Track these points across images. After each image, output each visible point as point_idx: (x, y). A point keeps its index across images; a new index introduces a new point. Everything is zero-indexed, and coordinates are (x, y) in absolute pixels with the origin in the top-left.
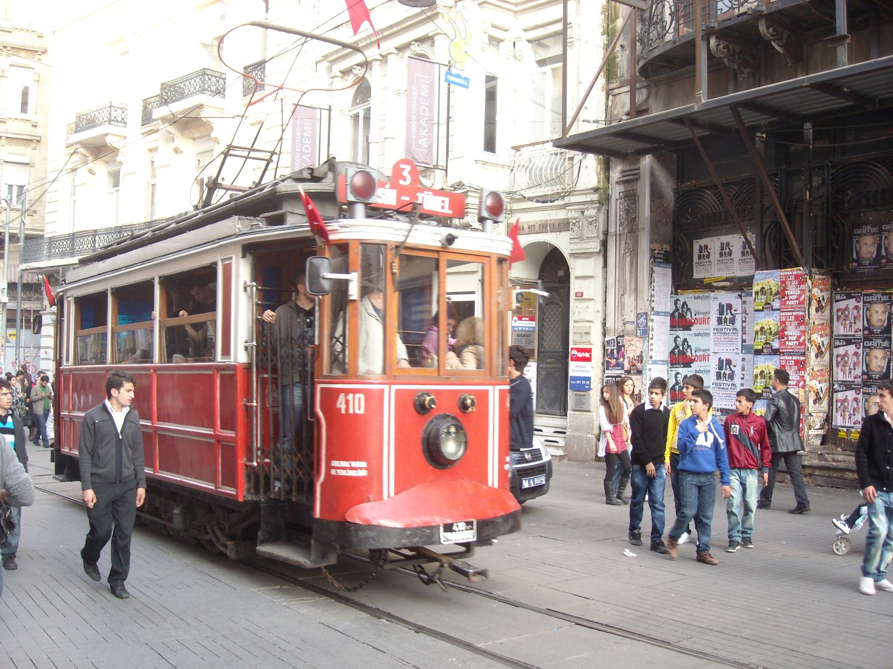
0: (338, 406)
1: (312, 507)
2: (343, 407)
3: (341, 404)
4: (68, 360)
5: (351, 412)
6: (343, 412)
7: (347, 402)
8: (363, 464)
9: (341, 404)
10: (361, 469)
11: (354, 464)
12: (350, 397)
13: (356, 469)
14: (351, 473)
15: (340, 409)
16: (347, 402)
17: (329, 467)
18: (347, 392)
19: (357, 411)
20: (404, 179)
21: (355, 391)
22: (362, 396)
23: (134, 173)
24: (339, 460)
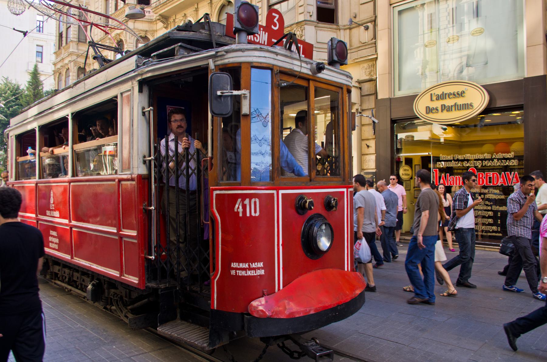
0: (236, 210)
1: (210, 297)
2: (241, 210)
3: (238, 208)
4: (12, 177)
5: (248, 215)
6: (241, 215)
7: (244, 207)
8: (261, 265)
9: (238, 207)
10: (259, 268)
11: (254, 265)
12: (247, 202)
13: (254, 269)
14: (249, 273)
15: (238, 213)
16: (244, 207)
17: (227, 267)
18: (244, 197)
19: (253, 214)
20: (275, 26)
21: (251, 196)
22: (257, 200)
24: (239, 262)
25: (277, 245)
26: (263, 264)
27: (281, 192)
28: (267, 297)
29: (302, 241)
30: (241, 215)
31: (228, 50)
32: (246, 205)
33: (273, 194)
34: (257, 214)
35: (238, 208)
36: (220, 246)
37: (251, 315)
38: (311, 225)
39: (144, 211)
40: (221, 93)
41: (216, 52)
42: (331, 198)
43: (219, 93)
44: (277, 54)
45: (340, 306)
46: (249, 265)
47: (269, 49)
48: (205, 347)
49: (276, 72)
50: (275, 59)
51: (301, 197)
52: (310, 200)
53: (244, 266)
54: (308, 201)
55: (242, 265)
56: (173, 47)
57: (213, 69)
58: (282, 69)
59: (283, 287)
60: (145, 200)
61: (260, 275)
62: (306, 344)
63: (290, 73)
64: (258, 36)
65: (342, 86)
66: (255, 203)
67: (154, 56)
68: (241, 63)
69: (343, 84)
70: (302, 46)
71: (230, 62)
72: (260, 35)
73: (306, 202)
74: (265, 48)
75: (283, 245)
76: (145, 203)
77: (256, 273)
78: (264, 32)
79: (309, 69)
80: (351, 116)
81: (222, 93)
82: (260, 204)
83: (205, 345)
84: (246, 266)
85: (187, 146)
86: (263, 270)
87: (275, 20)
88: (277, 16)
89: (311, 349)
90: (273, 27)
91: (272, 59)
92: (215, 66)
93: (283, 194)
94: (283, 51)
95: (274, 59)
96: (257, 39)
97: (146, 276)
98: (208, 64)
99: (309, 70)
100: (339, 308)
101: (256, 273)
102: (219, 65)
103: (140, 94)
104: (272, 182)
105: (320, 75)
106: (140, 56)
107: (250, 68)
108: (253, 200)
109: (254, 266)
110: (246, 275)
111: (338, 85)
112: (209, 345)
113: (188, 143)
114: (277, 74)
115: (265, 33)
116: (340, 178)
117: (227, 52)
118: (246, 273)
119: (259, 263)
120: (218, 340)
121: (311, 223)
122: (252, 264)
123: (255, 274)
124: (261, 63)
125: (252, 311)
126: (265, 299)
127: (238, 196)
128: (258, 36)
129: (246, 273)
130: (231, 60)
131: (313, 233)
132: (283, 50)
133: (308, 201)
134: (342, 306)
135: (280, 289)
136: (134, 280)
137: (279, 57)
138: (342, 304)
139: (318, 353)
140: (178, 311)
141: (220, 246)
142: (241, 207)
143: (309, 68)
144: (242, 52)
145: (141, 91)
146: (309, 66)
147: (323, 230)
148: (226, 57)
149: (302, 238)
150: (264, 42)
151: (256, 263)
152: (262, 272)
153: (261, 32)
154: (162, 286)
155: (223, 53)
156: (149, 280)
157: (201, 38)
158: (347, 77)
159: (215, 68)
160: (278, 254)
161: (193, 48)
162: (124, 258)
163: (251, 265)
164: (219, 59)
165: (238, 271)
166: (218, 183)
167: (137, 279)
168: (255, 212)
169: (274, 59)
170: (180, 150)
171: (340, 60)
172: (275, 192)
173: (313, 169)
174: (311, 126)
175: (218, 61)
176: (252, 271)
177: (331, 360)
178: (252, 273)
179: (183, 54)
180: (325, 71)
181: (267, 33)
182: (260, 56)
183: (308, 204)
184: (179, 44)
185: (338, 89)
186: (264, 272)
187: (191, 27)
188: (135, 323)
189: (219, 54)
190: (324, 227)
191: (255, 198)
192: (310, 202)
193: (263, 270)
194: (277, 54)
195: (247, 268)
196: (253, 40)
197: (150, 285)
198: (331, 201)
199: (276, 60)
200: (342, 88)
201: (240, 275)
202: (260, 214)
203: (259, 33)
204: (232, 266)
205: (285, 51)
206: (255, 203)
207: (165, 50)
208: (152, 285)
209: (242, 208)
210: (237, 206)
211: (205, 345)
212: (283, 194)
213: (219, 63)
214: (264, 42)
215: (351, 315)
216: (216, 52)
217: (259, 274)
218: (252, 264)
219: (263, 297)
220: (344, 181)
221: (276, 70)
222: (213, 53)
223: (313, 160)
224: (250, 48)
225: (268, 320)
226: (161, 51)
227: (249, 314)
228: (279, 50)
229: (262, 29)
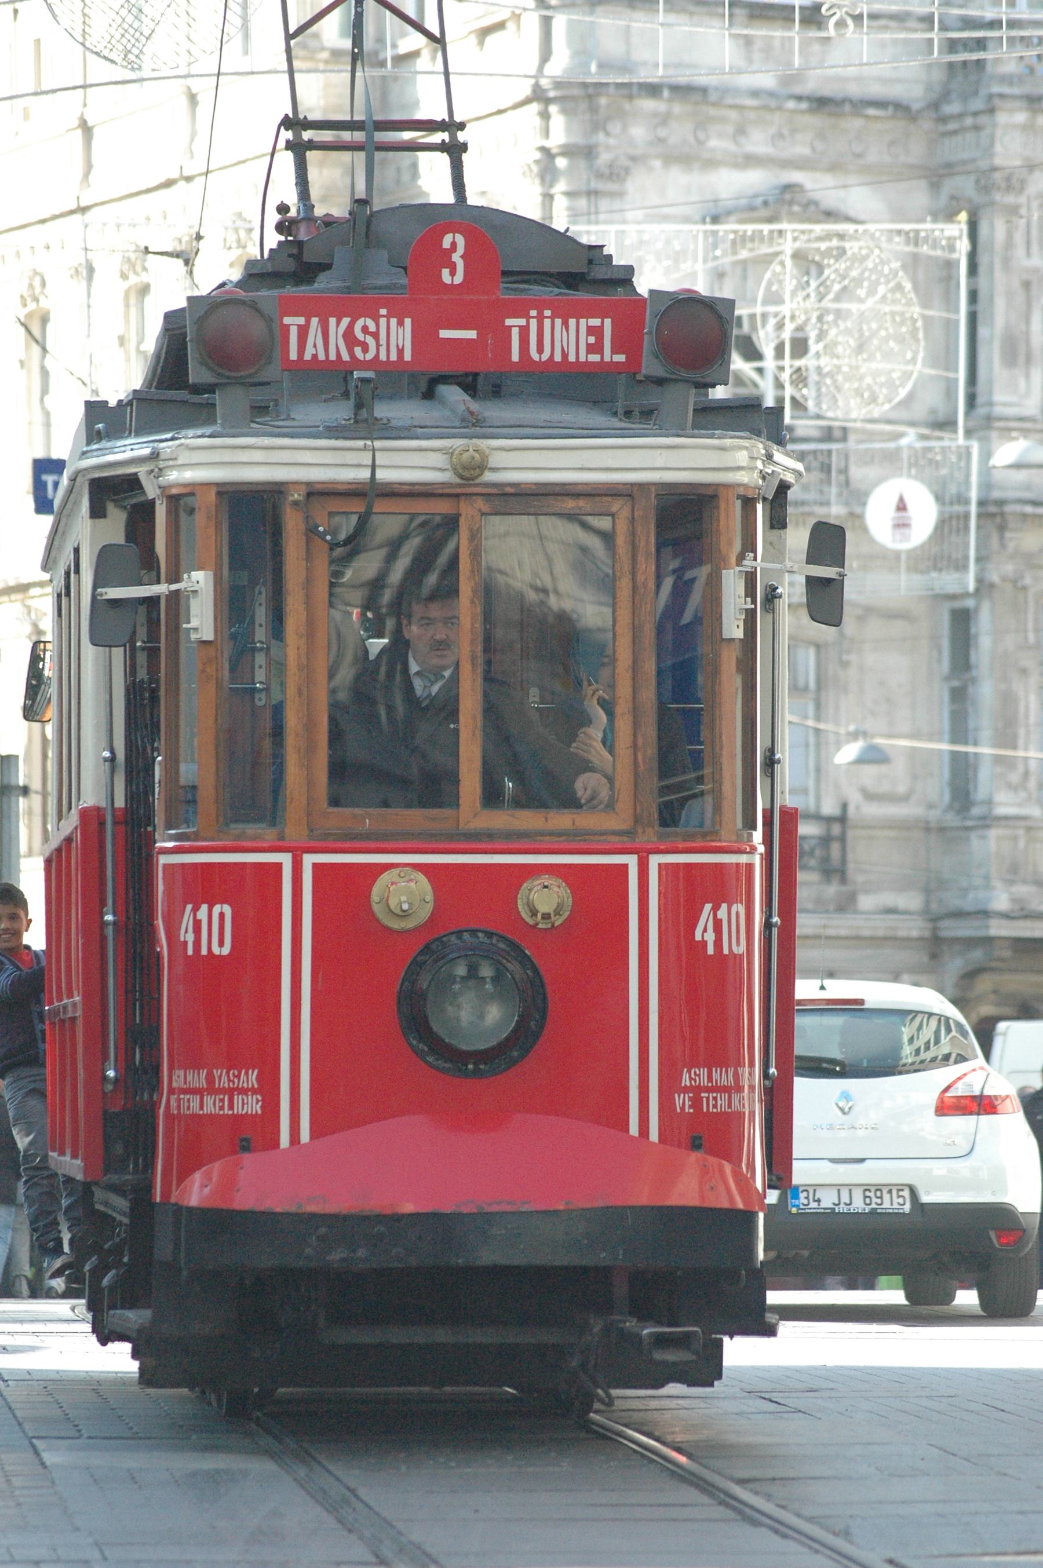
5: (204, 951)
7: (197, 924)
12: (203, 913)
16: (197, 924)
23: (38, 42)
32: (200, 921)
46: (210, 1079)
64: (370, 340)
70: (608, 322)
72: (376, 335)
78: (394, 321)
96: (365, 348)
115: (401, 323)
128: (370, 340)
150: (400, 352)
153: (383, 321)
181: (408, 322)
196: (346, 357)
203: (372, 328)
214: (400, 352)
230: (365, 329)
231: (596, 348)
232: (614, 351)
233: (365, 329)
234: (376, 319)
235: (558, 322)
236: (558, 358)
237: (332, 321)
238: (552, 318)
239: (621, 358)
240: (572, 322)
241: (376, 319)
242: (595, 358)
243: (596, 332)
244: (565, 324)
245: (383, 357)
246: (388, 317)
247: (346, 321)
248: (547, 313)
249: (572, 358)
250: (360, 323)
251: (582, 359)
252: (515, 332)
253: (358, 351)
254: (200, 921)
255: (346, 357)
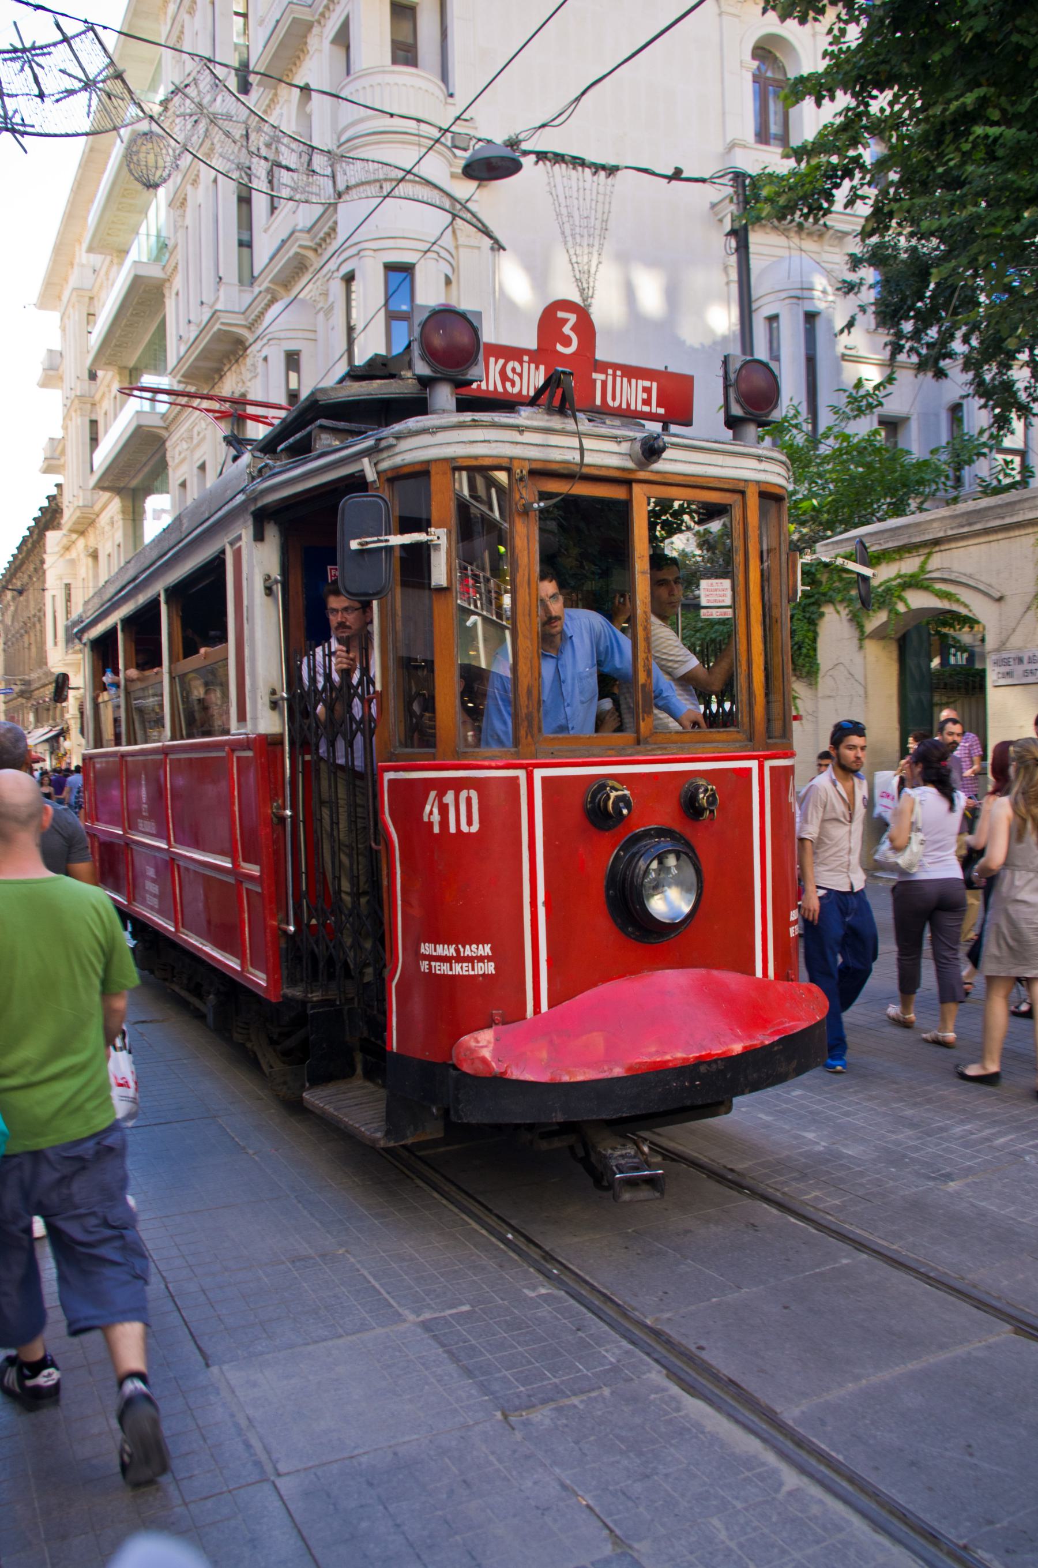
0: (426, 819)
2: (436, 818)
3: (431, 813)
5: (453, 829)
6: (436, 830)
7: (444, 809)
8: (486, 950)
9: (431, 812)
10: (481, 959)
11: (468, 951)
12: (449, 798)
13: (470, 959)
14: (458, 969)
15: (430, 824)
16: (444, 809)
18: (442, 786)
19: (464, 828)
20: (567, 342)
21: (458, 785)
22: (474, 794)
24: (436, 941)
25: (531, 903)
26: (491, 948)
27: (539, 774)
28: (500, 1027)
29: (608, 896)
30: (436, 830)
31: (400, 432)
32: (447, 805)
33: (517, 778)
34: (475, 828)
35: (431, 813)
36: (399, 902)
37: (459, 1070)
38: (634, 855)
39: (275, 820)
40: (361, 544)
41: (377, 440)
42: (697, 788)
43: (354, 545)
44: (520, 429)
45: (709, 1064)
46: (457, 951)
47: (496, 419)
48: (379, 1139)
49: (517, 477)
50: (517, 443)
51: (601, 784)
52: (620, 793)
53: (446, 953)
54: (613, 794)
55: (443, 950)
56: (309, 429)
57: (375, 481)
58: (534, 466)
59: (550, 1006)
60: (276, 795)
61: (484, 975)
62: (610, 1151)
63: (565, 472)
64: (517, 379)
65: (741, 486)
66: (469, 800)
67: (282, 451)
68: (428, 462)
69: (745, 481)
70: (655, 385)
71: (406, 462)
72: (520, 375)
73: (608, 797)
74: (483, 419)
75: (547, 903)
76: (277, 801)
77: (473, 969)
78: (533, 366)
79: (626, 454)
80: (784, 565)
81: (361, 544)
82: (480, 803)
83: (379, 1135)
84: (451, 951)
85: (345, 666)
86: (492, 964)
87: (567, 330)
88: (572, 318)
89: (613, 1163)
90: (559, 348)
91: (507, 445)
92: (378, 473)
93: (545, 780)
94: (542, 420)
95: (512, 443)
96: (513, 385)
97: (285, 973)
98: (363, 471)
99: (628, 458)
100: (703, 1069)
101: (473, 969)
102: (385, 471)
103: (259, 545)
104: (513, 750)
105: (659, 466)
106: (258, 454)
107: (450, 472)
108: (464, 794)
109: (468, 953)
110: (450, 973)
111: (726, 486)
112: (388, 1134)
113: (347, 658)
114: (521, 479)
115: (537, 368)
116: (738, 732)
117: (399, 437)
118: (451, 969)
119: (481, 946)
120: (412, 1127)
121: (634, 850)
122: (464, 947)
123: (472, 973)
124: (476, 458)
125: (458, 1059)
126: (496, 1034)
127: (430, 783)
128: (517, 379)
129: (451, 969)
130: (409, 458)
131: (632, 877)
132: (539, 416)
133: (613, 794)
134: (714, 1066)
135: (540, 1012)
136: (260, 979)
137: (529, 437)
138: (715, 1061)
139: (621, 1172)
140: (359, 1057)
141: (399, 902)
142: (436, 811)
143: (623, 451)
144: (18, 545)
145: (259, 537)
146: (625, 447)
147: (669, 868)
148: (397, 450)
149: (608, 889)
151: (474, 946)
152: (490, 968)
153: (525, 365)
154: (316, 996)
155: (392, 441)
156: (293, 982)
157: (401, 391)
158: (760, 461)
159: (379, 478)
160: (532, 926)
161: (353, 426)
162: (247, 929)
163: (462, 950)
164: (385, 455)
165: (433, 964)
166: (393, 754)
167: (264, 976)
168: (470, 823)
169: (512, 443)
170: (336, 677)
171: (751, 414)
172: (521, 774)
173: (644, 712)
174: (638, 602)
175: (383, 460)
176: (465, 964)
177: (657, 1195)
178: (465, 969)
179: (330, 446)
180: (667, 454)
181: (542, 368)
182: (472, 439)
183: (613, 803)
184: (319, 422)
185: (728, 495)
186: (495, 969)
187: (384, 365)
188: (285, 1083)
189: (383, 444)
190: (671, 861)
191: (468, 789)
192: (617, 797)
193: (492, 964)
194: (520, 429)
195: (452, 957)
196: (500, 389)
197: (289, 992)
198: (697, 794)
199: (519, 446)
200: (743, 493)
201: (438, 972)
202: (480, 828)
203: (518, 370)
204: (422, 950)
205: (546, 417)
206: (469, 800)
207: (298, 436)
208: (296, 992)
209: (440, 813)
210: (428, 808)
211: (379, 1135)
212: (545, 780)
213: (384, 465)
215: (751, 1091)
216: (377, 440)
217: (481, 972)
218: (464, 947)
219: (489, 1026)
220: (751, 740)
221: (518, 471)
222: (370, 442)
223: (643, 691)
224: (446, 425)
225: (499, 1083)
226: (291, 440)
227: (455, 1067)
228: (528, 418)
229: (526, 358)
230: (514, 370)
231: (647, 402)
232: (658, 405)
233: (514, 370)
234: (521, 363)
235: (625, 380)
236: (624, 406)
237: (492, 360)
238: (622, 377)
239: (661, 411)
240: (633, 381)
241: (521, 363)
242: (646, 409)
243: (646, 390)
244: (629, 382)
245: (524, 393)
246: (529, 363)
247: (501, 362)
248: (619, 373)
249: (633, 407)
250: (510, 365)
251: (639, 409)
252: (599, 385)
253: (508, 385)
254: (447, 805)
255: (500, 389)
